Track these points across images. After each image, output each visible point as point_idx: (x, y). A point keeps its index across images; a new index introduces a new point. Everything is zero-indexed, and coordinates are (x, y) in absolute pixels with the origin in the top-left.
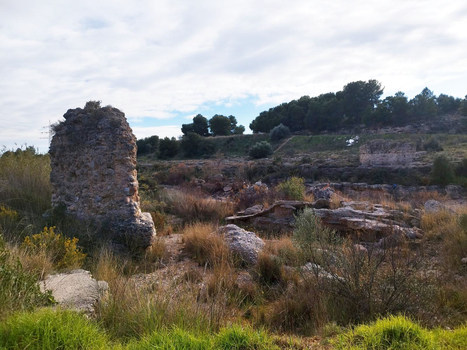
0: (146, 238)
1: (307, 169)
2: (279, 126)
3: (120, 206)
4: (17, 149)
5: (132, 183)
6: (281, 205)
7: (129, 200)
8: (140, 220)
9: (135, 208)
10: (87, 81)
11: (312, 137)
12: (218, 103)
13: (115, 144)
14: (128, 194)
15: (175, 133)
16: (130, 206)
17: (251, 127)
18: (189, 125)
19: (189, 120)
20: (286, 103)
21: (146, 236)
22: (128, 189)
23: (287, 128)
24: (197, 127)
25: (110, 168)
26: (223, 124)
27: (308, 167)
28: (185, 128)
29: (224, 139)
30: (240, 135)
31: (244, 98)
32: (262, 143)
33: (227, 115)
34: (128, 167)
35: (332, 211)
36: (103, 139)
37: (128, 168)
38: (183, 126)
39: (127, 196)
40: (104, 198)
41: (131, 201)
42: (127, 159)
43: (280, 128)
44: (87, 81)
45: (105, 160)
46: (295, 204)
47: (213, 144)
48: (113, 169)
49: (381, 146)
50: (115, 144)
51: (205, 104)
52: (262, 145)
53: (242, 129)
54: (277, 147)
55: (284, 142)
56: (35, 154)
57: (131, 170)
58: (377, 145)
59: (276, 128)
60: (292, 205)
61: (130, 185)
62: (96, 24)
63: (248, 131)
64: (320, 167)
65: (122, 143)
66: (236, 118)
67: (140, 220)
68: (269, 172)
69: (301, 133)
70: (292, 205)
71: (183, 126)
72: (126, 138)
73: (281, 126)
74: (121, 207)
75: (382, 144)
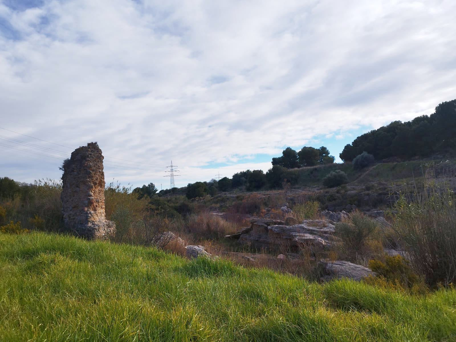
0: (90, 236)
1: (367, 196)
2: (362, 154)
3: (82, 213)
4: (143, 186)
5: (89, 197)
6: (255, 222)
7: (86, 209)
8: (92, 223)
9: (90, 215)
10: (210, 127)
11: (397, 164)
12: (328, 136)
13: (80, 171)
14: (87, 205)
15: (266, 167)
16: (87, 213)
17: (342, 156)
18: (279, 158)
19: (279, 154)
20: (375, 130)
21: (90, 234)
22: (86, 202)
23: (371, 156)
24: (288, 159)
25: (78, 187)
26: (313, 156)
27: (368, 195)
28: (275, 161)
29: (308, 170)
30: (330, 164)
31: (334, 130)
32: (336, 172)
33: (317, 146)
34: (88, 186)
35: (286, 227)
36: (75, 168)
37: (87, 187)
38: (274, 159)
39: (86, 206)
40: (73, 208)
41: (88, 210)
42: (87, 181)
43: (363, 156)
44: (210, 127)
45: (74, 182)
46: (266, 221)
47: (295, 175)
48: (80, 188)
49: (445, 170)
50: (80, 171)
51: (315, 138)
52: (336, 174)
53: (332, 159)
54: (360, 176)
55: (367, 170)
56: (155, 189)
57: (90, 189)
58: (442, 169)
59: (359, 156)
60: (264, 223)
61: (88, 198)
62: (219, 79)
63: (338, 161)
64: (380, 194)
65: (84, 170)
66: (328, 149)
67: (92, 223)
68: (330, 201)
69: (389, 160)
70: (264, 223)
71: (274, 159)
72: (86, 166)
73: (365, 154)
74: (82, 214)
75: (447, 167)
